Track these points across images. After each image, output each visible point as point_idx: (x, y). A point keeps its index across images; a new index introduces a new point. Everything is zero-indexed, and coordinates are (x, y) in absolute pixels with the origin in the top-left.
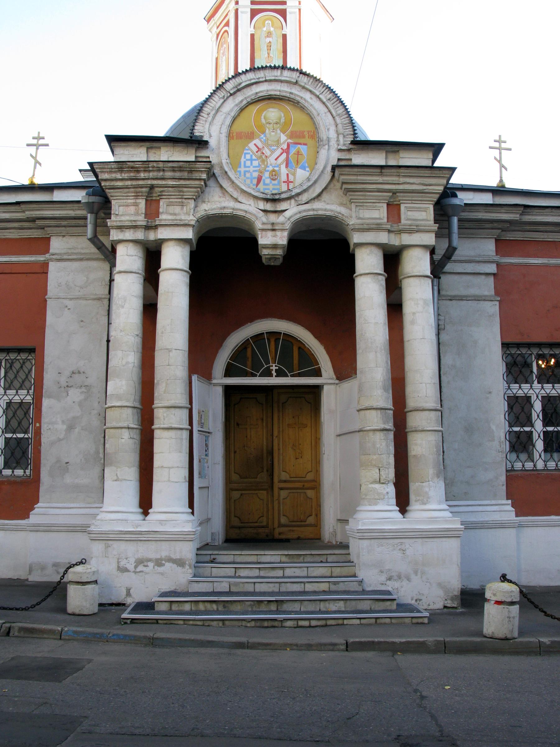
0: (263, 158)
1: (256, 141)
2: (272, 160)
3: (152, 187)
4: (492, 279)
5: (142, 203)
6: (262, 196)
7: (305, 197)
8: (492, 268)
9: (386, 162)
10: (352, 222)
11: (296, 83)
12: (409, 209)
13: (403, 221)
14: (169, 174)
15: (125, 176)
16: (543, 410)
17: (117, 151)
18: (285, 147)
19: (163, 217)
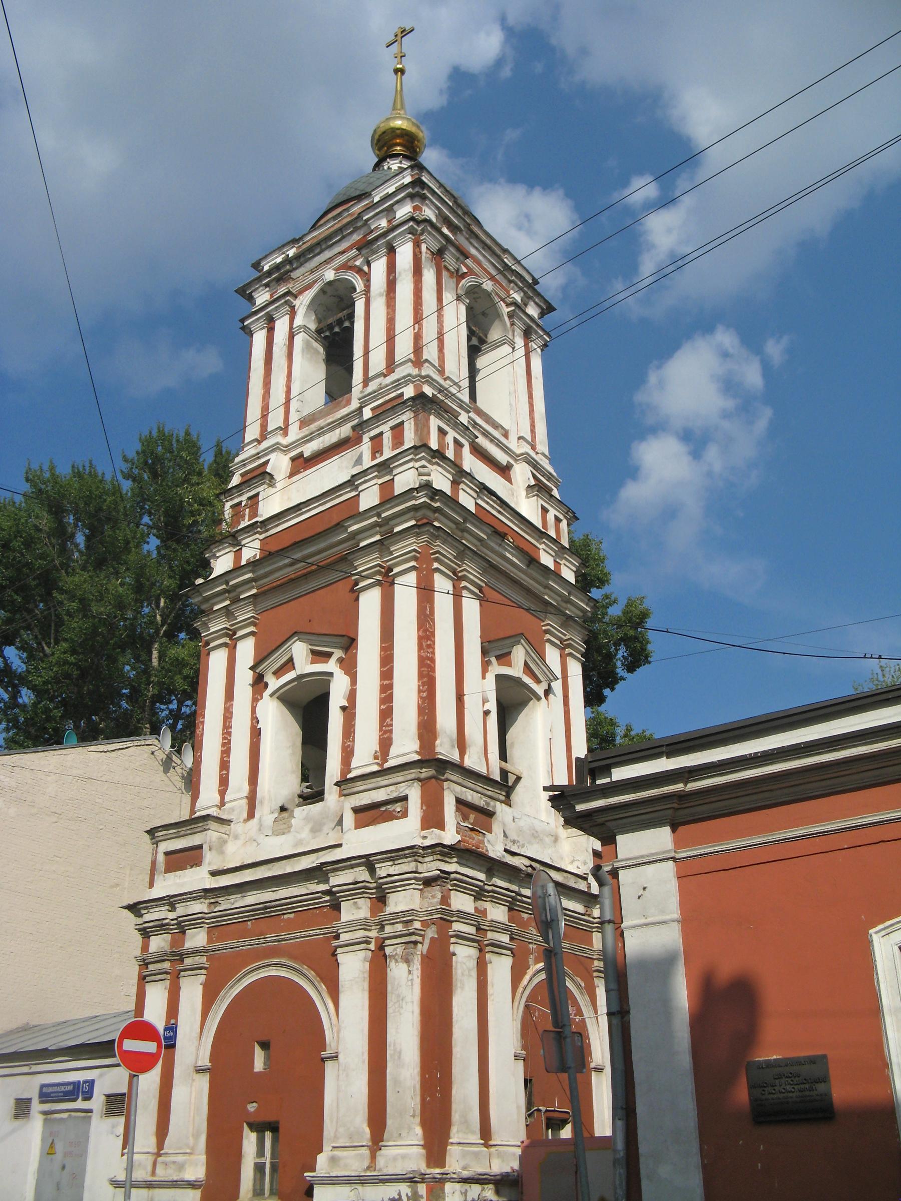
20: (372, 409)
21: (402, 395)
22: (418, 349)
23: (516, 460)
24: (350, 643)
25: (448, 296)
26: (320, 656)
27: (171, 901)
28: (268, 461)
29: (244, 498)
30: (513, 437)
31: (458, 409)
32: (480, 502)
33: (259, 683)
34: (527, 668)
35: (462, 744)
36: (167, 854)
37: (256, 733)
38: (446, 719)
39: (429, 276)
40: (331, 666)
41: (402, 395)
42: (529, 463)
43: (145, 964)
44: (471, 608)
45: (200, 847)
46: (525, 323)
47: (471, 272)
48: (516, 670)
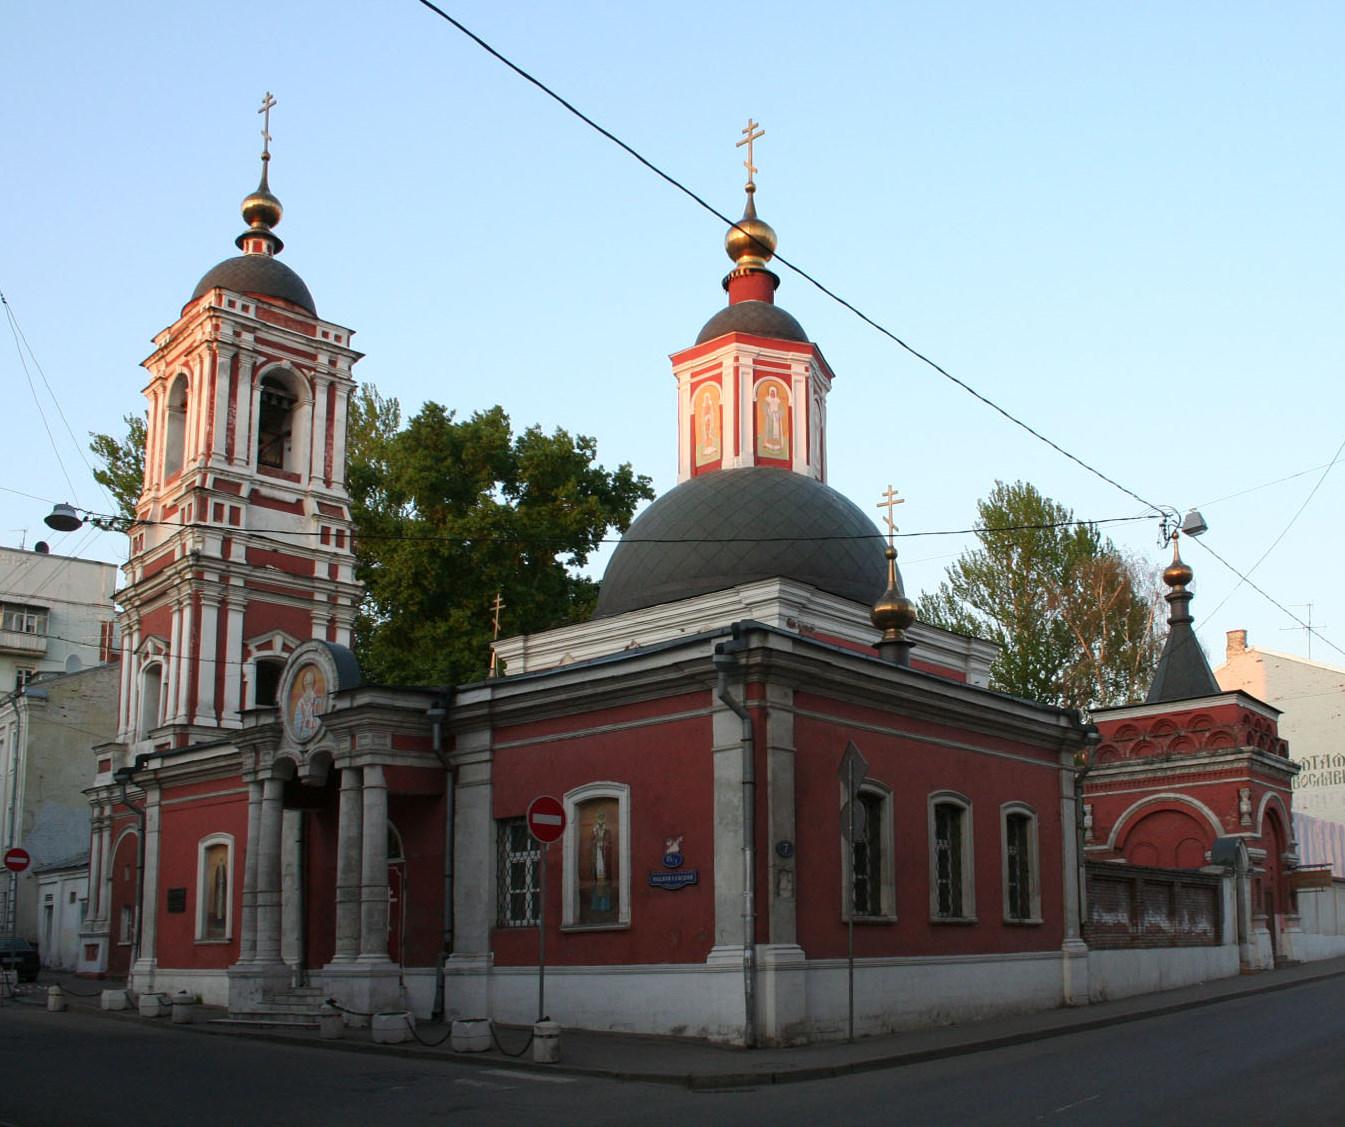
0: (303, 713)
1: (302, 700)
2: (307, 714)
3: (254, 745)
4: (489, 765)
5: (253, 754)
6: (298, 741)
7: (320, 736)
8: (487, 756)
9: (352, 703)
10: (335, 753)
11: (316, 651)
12: (361, 738)
13: (357, 748)
14: (257, 735)
15: (241, 739)
16: (524, 877)
17: (246, 721)
18: (312, 701)
19: (262, 764)
20: (187, 486)
21: (194, 482)
22: (209, 446)
23: (305, 496)
24: (168, 645)
25: (243, 390)
26: (158, 651)
27: (97, 790)
28: (149, 510)
29: (138, 535)
30: (305, 479)
31: (240, 481)
32: (251, 545)
33: (140, 664)
34: (286, 648)
35: (219, 704)
36: (101, 762)
37: (138, 692)
38: (206, 693)
39: (223, 383)
40: (160, 658)
41: (194, 482)
42: (314, 497)
43: (93, 823)
44: (235, 622)
45: (109, 760)
46: (327, 380)
47: (271, 358)
48: (277, 651)
